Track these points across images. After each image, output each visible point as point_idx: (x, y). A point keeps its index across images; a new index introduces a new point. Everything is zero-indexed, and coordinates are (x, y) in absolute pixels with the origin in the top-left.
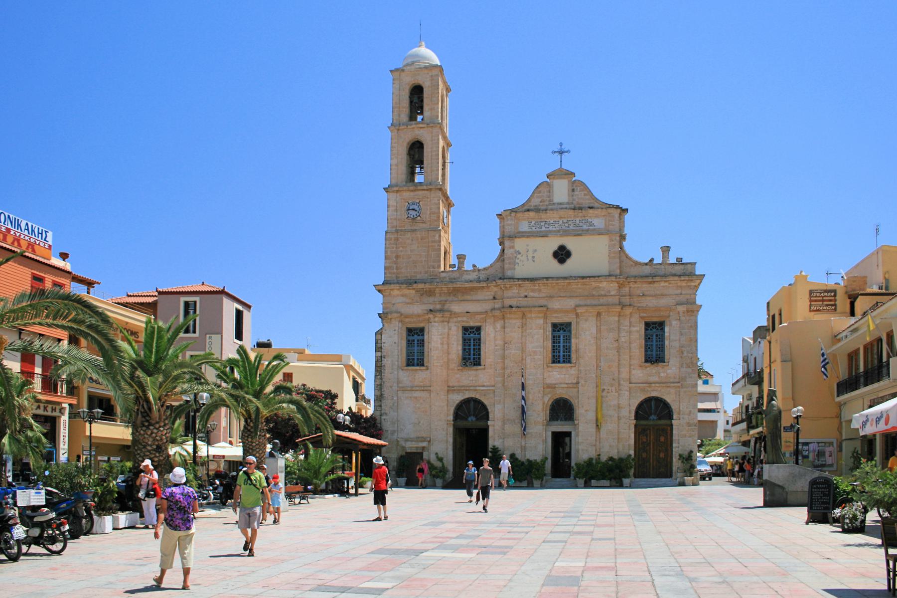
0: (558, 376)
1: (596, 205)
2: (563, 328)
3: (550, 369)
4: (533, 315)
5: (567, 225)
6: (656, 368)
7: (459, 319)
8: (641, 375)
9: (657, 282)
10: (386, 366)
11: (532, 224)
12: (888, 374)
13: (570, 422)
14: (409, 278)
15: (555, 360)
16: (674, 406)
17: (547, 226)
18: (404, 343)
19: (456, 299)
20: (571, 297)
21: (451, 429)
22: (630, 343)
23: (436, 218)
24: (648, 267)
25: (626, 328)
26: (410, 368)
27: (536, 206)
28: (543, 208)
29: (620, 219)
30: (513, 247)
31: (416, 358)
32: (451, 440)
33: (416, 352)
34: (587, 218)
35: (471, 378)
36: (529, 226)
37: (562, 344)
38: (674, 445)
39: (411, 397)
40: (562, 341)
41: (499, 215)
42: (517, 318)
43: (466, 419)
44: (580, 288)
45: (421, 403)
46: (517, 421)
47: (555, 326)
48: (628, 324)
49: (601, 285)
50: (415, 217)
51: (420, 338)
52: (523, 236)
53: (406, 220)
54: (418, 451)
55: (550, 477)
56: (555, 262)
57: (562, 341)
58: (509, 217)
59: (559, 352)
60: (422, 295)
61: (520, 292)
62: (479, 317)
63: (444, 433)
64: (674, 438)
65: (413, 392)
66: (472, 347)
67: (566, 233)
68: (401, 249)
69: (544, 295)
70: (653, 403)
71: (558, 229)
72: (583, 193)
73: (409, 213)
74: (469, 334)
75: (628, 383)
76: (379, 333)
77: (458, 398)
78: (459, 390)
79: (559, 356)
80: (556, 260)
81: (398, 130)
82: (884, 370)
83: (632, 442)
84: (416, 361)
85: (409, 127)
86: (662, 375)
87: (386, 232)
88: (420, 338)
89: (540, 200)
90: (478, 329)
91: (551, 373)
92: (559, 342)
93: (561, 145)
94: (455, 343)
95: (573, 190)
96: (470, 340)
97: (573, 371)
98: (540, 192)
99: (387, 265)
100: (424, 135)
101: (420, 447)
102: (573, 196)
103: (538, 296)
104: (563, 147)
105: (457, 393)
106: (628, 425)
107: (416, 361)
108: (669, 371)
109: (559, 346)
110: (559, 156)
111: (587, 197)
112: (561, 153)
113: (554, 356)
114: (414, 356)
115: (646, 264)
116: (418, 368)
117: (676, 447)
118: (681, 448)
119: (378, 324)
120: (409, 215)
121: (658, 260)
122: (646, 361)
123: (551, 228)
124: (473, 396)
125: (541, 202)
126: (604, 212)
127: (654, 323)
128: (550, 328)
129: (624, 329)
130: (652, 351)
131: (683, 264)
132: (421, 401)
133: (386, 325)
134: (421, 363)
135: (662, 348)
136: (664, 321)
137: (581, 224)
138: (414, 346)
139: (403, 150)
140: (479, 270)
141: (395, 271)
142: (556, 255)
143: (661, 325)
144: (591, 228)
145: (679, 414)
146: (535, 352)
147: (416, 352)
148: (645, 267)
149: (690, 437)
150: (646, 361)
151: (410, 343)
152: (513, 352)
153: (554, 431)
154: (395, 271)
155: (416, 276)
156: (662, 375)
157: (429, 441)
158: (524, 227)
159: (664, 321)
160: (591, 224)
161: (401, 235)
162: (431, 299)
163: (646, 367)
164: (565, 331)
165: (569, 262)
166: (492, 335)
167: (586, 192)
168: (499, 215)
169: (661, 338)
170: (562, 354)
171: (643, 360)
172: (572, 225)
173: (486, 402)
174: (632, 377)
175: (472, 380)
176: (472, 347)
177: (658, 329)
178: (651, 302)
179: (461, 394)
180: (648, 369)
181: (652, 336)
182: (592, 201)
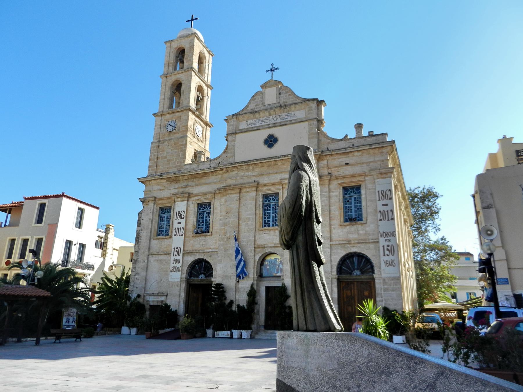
0: (268, 237)
1: (298, 101)
2: (273, 198)
3: (261, 232)
4: (248, 190)
5: (275, 119)
6: (355, 226)
7: (196, 198)
8: (342, 233)
9: (351, 152)
10: (142, 237)
11: (249, 123)
17: (260, 122)
18: (156, 219)
19: (194, 184)
20: (277, 173)
21: (183, 286)
22: (330, 206)
23: (185, 129)
24: (343, 142)
25: (325, 193)
26: (159, 237)
27: (252, 109)
28: (256, 110)
29: (318, 109)
32: (183, 294)
35: (201, 243)
36: (248, 124)
37: (271, 211)
39: (157, 260)
40: (272, 208)
41: (226, 120)
42: (235, 193)
43: (198, 277)
45: (164, 265)
46: (232, 277)
47: (265, 197)
48: (328, 190)
50: (172, 130)
51: (168, 215)
52: (242, 132)
53: (166, 133)
54: (159, 304)
55: (263, 329)
56: (265, 147)
57: (272, 208)
58: (232, 120)
59: (269, 218)
61: (238, 173)
62: (209, 196)
63: (178, 288)
64: (377, 292)
65: (159, 256)
66: (205, 219)
67: (274, 125)
68: (161, 152)
70: (355, 259)
71: (268, 123)
72: (287, 94)
73: (168, 128)
74: (203, 209)
75: (329, 240)
76: (140, 213)
77: (190, 259)
78: (191, 253)
79: (269, 221)
80: (266, 146)
81: (167, 77)
85: (173, 74)
86: (361, 232)
87: (152, 143)
88: (168, 215)
89: (255, 105)
90: (209, 204)
91: (261, 236)
92: (270, 210)
93: (272, 65)
94: (192, 216)
95: (280, 94)
96: (203, 213)
98: (255, 99)
99: (150, 164)
101: (160, 301)
102: (279, 98)
103: (251, 174)
104: (274, 66)
105: (190, 255)
106: (330, 279)
108: (367, 229)
109: (270, 213)
110: (271, 73)
111: (291, 97)
113: (265, 221)
115: (341, 140)
117: (380, 301)
118: (384, 302)
119: (140, 206)
120: (168, 130)
121: (352, 134)
122: (346, 221)
123: (263, 124)
125: (255, 106)
126: (304, 105)
127: (352, 188)
128: (260, 198)
129: (324, 195)
130: (351, 212)
131: (375, 135)
132: (164, 263)
133: (145, 206)
134: (167, 233)
135: (359, 209)
136: (360, 185)
137: (286, 117)
138: (164, 221)
139: (168, 89)
140: (211, 161)
143: (358, 188)
144: (294, 118)
146: (249, 219)
148: (340, 142)
149: (393, 291)
150: (346, 221)
151: (161, 219)
152: (232, 219)
153: (267, 286)
155: (169, 170)
156: (361, 232)
157: (167, 296)
158: (243, 125)
159: (360, 185)
160: (294, 115)
162: (177, 185)
163: (346, 226)
164: (274, 200)
165: (276, 146)
166: (219, 208)
167: (290, 93)
168: (226, 120)
169: (359, 201)
170: (271, 219)
171: (343, 220)
172: (279, 118)
173: (211, 262)
174: (333, 235)
175: (202, 245)
177: (356, 193)
178: (348, 171)
179: (193, 256)
180: (348, 227)
181: (351, 199)
182: (295, 99)
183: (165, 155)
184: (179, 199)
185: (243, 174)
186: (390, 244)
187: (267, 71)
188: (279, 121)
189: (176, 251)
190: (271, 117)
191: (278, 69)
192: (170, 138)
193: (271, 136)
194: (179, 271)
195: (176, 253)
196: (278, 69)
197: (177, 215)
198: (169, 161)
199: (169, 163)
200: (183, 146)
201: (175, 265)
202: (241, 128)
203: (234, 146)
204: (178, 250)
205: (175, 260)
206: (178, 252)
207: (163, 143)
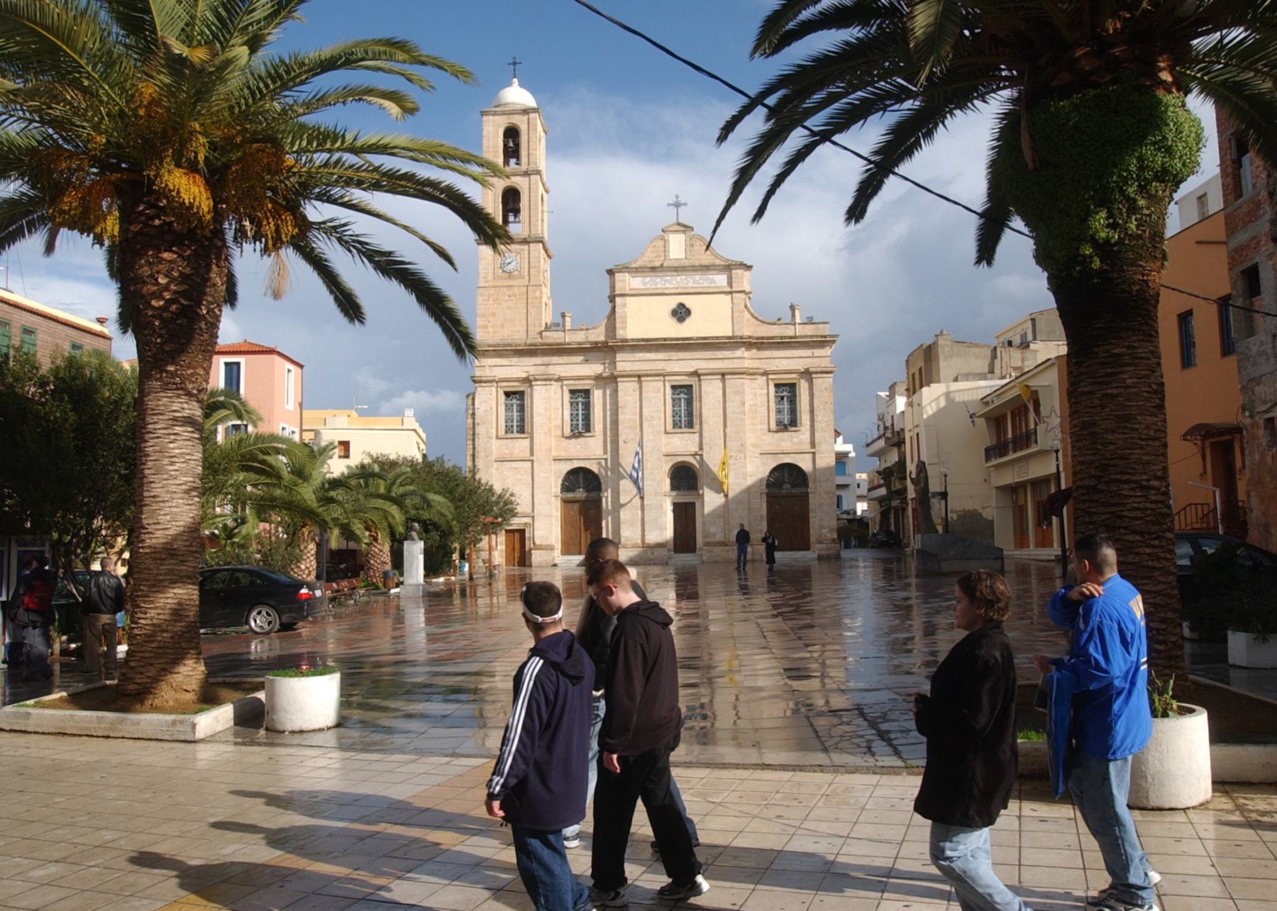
1: (718, 262)
4: (650, 378)
12: (1036, 442)
13: (694, 492)
18: (502, 409)
26: (510, 435)
28: (657, 264)
30: (624, 305)
38: (811, 515)
56: (673, 321)
82: (1033, 437)
83: (764, 512)
86: (795, 440)
93: (677, 197)
95: (692, 245)
100: (519, 182)
112: (677, 205)
116: (518, 435)
123: (668, 285)
124: (583, 465)
128: (669, 391)
134: (522, 430)
142: (674, 313)
145: (815, 481)
151: (508, 408)
152: (628, 417)
165: (688, 320)
176: (580, 412)
184: (539, 383)
187: (669, 205)
188: (690, 285)
190: (678, 278)
191: (685, 204)
192: (510, 284)
193: (682, 305)
196: (685, 204)
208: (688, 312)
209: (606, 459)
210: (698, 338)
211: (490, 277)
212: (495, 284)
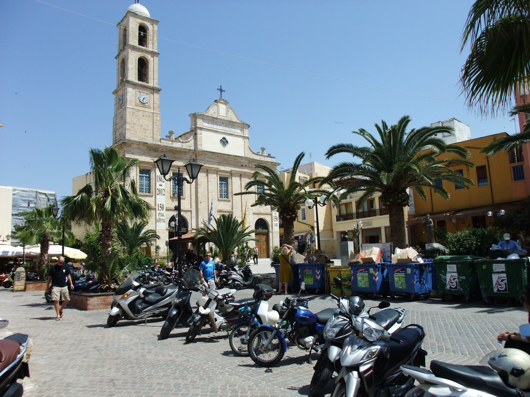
14: (142, 139)
15: (221, 197)
16: (270, 223)
31: (144, 187)
33: (144, 184)
34: (234, 126)
44: (232, 161)
49: (242, 161)
50: (145, 103)
58: (199, 117)
60: (150, 150)
68: (136, 120)
69: (216, 161)
84: (144, 190)
89: (213, 112)
97: (230, 203)
98: (213, 108)
107: (144, 190)
112: (221, 90)
114: (143, 186)
141: (133, 132)
144: (236, 132)
147: (144, 184)
152: (202, 190)
154: (133, 132)
161: (136, 111)
164: (224, 182)
183: (141, 123)
185: (208, 159)
186: (276, 215)
189: (160, 207)
193: (224, 138)
194: (164, 222)
195: (160, 208)
197: (158, 179)
198: (145, 129)
199: (145, 132)
200: (158, 122)
201: (160, 217)
202: (204, 125)
203: (202, 137)
204: (161, 206)
205: (160, 213)
206: (162, 208)
207: (138, 112)
208: (227, 142)
209: (191, 211)
210: (234, 156)
211: (134, 104)
212: (135, 108)
